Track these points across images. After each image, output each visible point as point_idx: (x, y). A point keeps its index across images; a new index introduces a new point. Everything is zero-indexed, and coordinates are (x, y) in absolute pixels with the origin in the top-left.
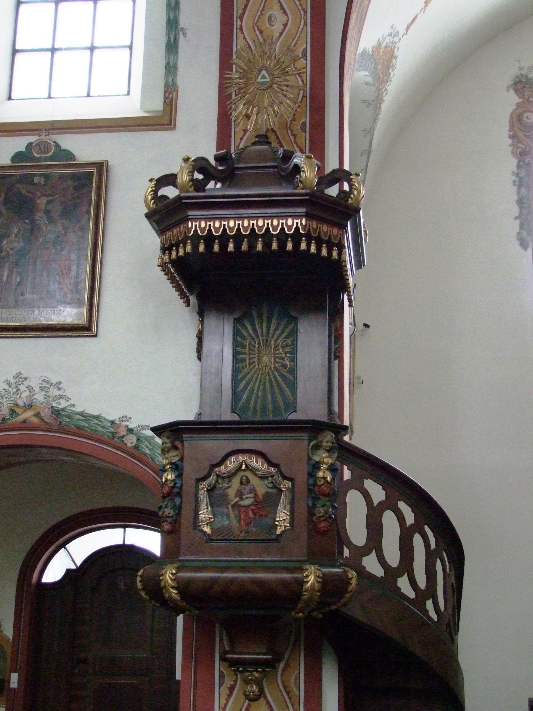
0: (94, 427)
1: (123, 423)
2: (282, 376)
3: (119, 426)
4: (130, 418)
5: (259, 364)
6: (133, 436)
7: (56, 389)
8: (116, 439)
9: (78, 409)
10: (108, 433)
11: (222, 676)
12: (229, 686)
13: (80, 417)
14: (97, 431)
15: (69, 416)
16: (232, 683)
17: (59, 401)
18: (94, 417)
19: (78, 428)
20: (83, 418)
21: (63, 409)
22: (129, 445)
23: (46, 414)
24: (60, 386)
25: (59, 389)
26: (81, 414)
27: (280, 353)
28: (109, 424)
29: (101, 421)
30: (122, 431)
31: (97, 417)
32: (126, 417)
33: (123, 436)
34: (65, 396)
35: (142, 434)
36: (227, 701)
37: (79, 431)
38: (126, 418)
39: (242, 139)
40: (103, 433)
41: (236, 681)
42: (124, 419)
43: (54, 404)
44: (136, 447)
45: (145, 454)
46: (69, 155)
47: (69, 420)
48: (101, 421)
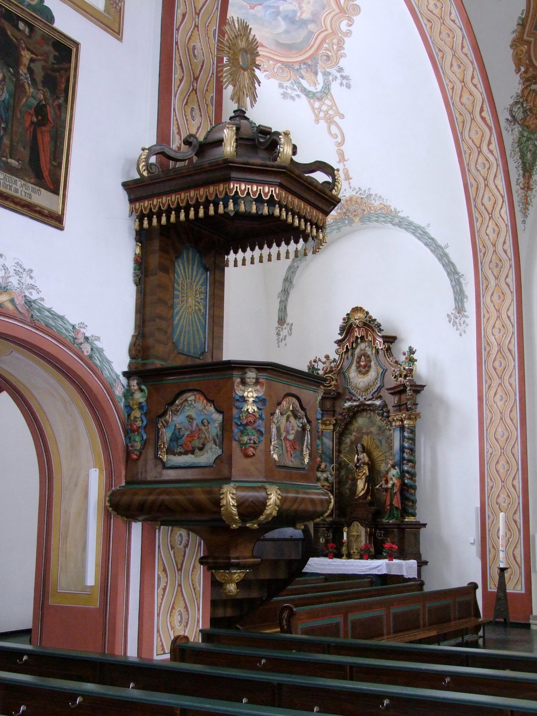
0: (59, 328)
1: (81, 329)
2: (199, 319)
3: (78, 332)
4: (86, 326)
5: (186, 303)
6: (88, 344)
7: (28, 277)
8: (75, 345)
9: (47, 304)
10: (70, 337)
11: (159, 578)
12: (163, 587)
13: (47, 313)
14: (62, 333)
15: (39, 310)
16: (165, 584)
17: (31, 290)
18: (59, 317)
20: (50, 315)
21: (34, 301)
22: (86, 354)
23: (19, 301)
24: (31, 275)
25: (31, 278)
26: (49, 311)
27: (197, 298)
28: (71, 328)
29: (65, 323)
31: (62, 318)
32: (83, 324)
33: (82, 343)
34: (36, 287)
35: (95, 344)
36: (162, 599)
37: (47, 330)
38: (83, 325)
39: (179, 87)
40: (67, 337)
41: (167, 583)
42: (82, 325)
43: (27, 294)
44: (91, 357)
45: (96, 365)
47: (39, 315)
48: (65, 323)
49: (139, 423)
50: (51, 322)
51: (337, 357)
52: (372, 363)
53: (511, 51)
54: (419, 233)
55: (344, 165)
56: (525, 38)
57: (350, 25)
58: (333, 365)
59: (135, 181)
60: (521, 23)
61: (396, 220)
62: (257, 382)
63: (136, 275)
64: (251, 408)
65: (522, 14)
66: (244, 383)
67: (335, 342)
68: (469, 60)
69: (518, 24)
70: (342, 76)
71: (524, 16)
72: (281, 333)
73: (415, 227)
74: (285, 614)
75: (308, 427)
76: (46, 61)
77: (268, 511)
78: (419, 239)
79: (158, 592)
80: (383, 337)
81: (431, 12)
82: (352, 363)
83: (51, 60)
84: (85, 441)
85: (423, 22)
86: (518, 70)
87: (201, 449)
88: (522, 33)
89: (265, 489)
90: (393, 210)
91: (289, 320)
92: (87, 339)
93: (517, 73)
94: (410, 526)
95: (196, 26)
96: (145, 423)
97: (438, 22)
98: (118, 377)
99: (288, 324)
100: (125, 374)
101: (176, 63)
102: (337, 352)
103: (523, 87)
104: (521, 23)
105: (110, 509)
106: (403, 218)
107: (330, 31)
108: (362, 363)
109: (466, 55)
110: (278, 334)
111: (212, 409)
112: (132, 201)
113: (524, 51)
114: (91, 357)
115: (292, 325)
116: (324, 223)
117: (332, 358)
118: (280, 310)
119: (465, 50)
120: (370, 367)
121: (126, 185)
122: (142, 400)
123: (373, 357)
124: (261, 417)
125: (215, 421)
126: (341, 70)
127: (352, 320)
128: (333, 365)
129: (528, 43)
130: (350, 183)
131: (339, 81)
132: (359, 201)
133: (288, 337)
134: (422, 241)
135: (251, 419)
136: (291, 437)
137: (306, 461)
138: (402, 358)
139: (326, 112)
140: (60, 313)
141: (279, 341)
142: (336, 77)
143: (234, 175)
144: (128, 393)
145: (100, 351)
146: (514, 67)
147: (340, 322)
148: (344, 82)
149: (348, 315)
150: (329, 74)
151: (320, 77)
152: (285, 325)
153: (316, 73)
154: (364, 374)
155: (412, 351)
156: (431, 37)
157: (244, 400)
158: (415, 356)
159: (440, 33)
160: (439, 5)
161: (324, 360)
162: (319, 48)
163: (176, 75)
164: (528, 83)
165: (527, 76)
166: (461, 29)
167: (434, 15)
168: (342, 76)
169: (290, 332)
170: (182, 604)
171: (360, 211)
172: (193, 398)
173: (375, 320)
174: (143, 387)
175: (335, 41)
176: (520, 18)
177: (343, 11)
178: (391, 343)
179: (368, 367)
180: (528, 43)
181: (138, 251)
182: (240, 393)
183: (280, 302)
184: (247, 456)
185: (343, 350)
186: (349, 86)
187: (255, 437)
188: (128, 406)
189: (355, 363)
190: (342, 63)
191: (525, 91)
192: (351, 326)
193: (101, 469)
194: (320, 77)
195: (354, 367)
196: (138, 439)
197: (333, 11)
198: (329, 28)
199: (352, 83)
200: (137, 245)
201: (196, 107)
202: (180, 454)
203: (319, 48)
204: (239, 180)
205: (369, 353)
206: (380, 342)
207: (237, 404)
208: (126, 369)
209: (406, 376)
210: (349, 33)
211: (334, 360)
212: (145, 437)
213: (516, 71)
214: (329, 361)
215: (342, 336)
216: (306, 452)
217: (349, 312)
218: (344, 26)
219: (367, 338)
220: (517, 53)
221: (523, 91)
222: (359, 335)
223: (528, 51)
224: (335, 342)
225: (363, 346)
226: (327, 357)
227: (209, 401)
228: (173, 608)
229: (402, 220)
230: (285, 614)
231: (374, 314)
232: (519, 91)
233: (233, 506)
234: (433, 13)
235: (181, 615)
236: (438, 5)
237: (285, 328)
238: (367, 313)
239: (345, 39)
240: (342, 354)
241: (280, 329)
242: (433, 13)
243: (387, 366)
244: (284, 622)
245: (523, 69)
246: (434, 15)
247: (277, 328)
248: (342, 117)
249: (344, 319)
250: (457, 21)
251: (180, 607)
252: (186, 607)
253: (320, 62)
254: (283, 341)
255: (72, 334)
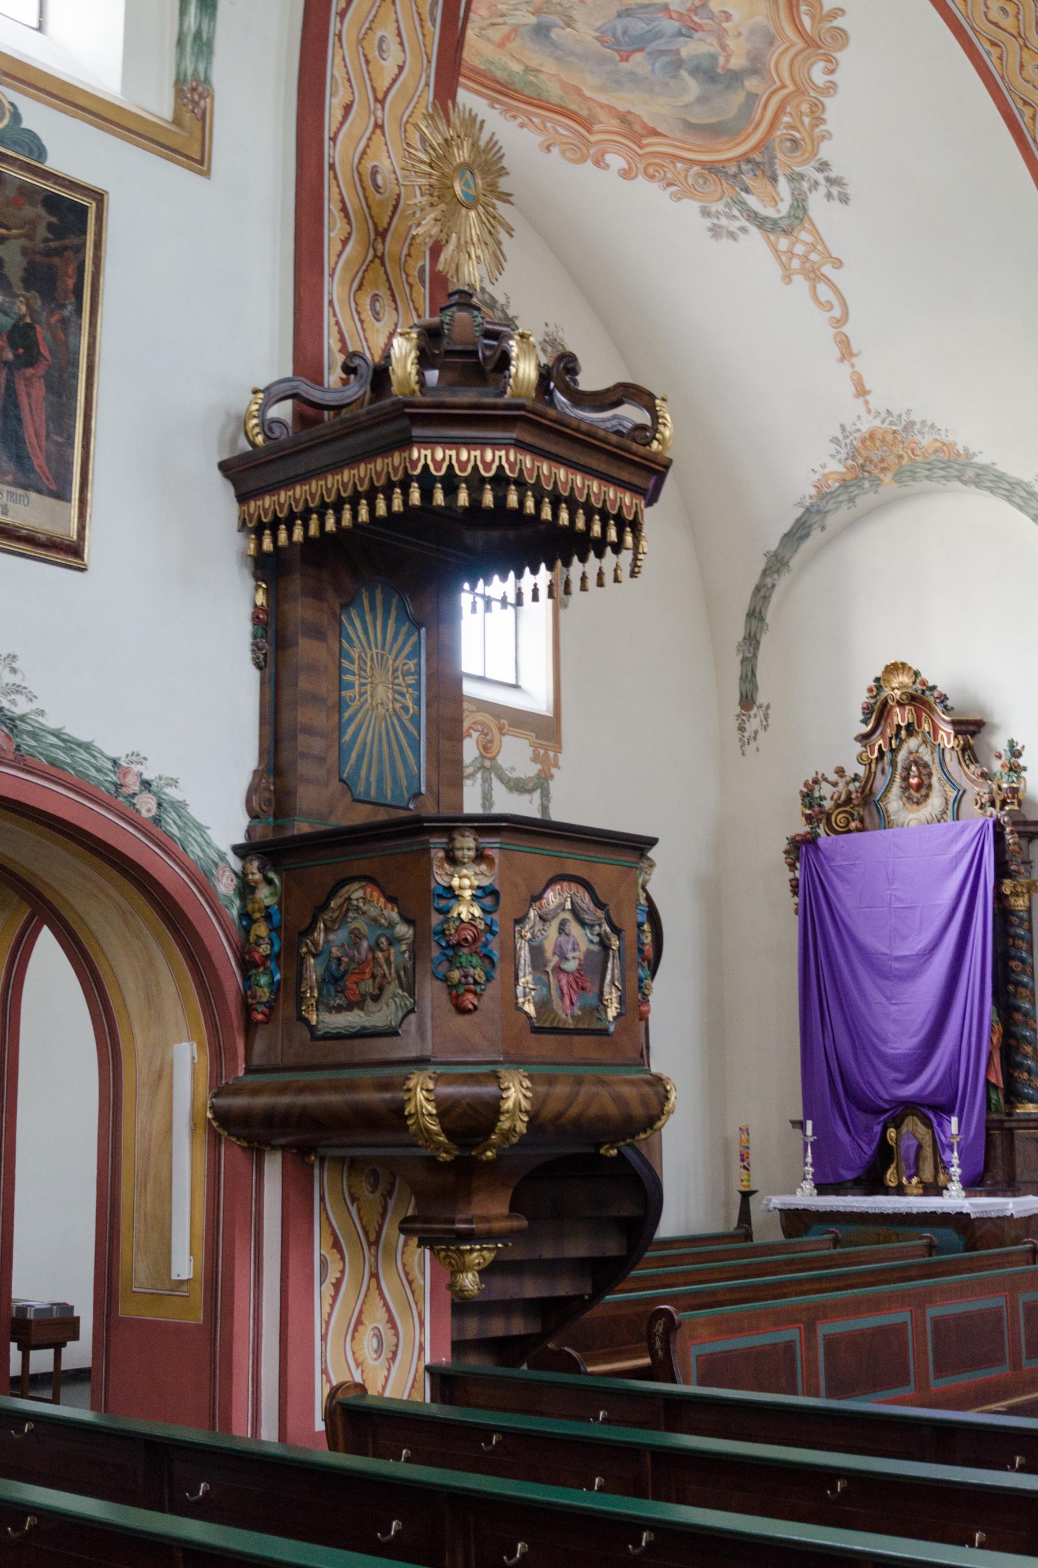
0: (82, 766)
1: (132, 766)
2: (403, 727)
3: (126, 773)
4: (145, 759)
5: (372, 697)
6: (150, 795)
7: (7, 670)
8: (121, 799)
9: (51, 722)
10: (107, 784)
11: (324, 1263)
12: (334, 1281)
14: (88, 776)
15: (34, 735)
16: (338, 1275)
17: (13, 696)
18: (80, 745)
19: (53, 763)
20: (62, 744)
21: (23, 718)
22: (145, 814)
24: (14, 665)
25: (14, 671)
26: (57, 734)
27: (400, 685)
28: (109, 765)
29: (94, 757)
30: (133, 785)
31: (87, 747)
32: (138, 755)
33: (134, 795)
34: (25, 688)
35: (165, 794)
36: (332, 1306)
37: (53, 771)
38: (137, 758)
39: (339, 256)
40: (100, 782)
41: (342, 1272)
42: (134, 758)
44: (157, 820)
45: (171, 836)
46: (35, 147)
47: (34, 743)
48: (94, 757)
49: (264, 949)
50: (62, 756)
51: (861, 771)
52: (934, 780)
54: (1021, 497)
55: (853, 366)
57: (832, 72)
58: (852, 787)
59: (244, 457)
61: (970, 473)
62: (480, 857)
63: (256, 648)
64: (466, 910)
66: (452, 860)
67: (856, 739)
70: (828, 180)
72: (747, 726)
73: (1010, 484)
74: (659, 1327)
75: (615, 943)
76: (29, 237)
77: (505, 1124)
78: (1020, 508)
79: (322, 1293)
80: (954, 723)
81: (996, 25)
82: (892, 781)
83: (42, 232)
84: (169, 988)
85: (982, 46)
87: (376, 998)
89: (496, 1077)
90: (962, 452)
91: (761, 698)
92: (146, 784)
94: (1023, 1124)
95: (379, 126)
96: (276, 948)
97: (1013, 46)
98: (222, 856)
99: (760, 707)
100: (237, 850)
101: (331, 207)
102: (860, 759)
105: (215, 1124)
106: (983, 467)
107: (791, 88)
108: (914, 781)
110: (742, 729)
111: (395, 915)
112: (242, 498)
114: (157, 820)
115: (768, 707)
116: (636, 513)
117: (850, 774)
118: (743, 679)
120: (930, 786)
121: (224, 467)
122: (268, 902)
123: (935, 769)
124: (489, 929)
125: (400, 940)
126: (824, 166)
127: (887, 692)
128: (852, 787)
130: (866, 402)
131: (822, 190)
132: (889, 438)
133: (761, 734)
134: (1028, 514)
135: (469, 935)
136: (571, 966)
137: (612, 1012)
138: (997, 766)
139: (805, 258)
140: (83, 737)
141: (744, 743)
142: (816, 183)
143: (417, 432)
144: (245, 889)
145: (179, 807)
147: (862, 697)
148: (835, 190)
149: (877, 680)
150: (802, 177)
151: (784, 187)
152: (755, 708)
153: (774, 179)
154: (918, 803)
155: (1016, 753)
156: (1002, 78)
157: (451, 893)
158: (1021, 761)
159: (1022, 66)
160: (1010, 8)
161: (833, 777)
162: (773, 125)
163: (334, 229)
167: (1004, 30)
168: (828, 180)
169: (765, 723)
170: (381, 1314)
171: (892, 460)
172: (360, 894)
173: (933, 688)
174: (272, 875)
175: (805, 107)
177: (811, 43)
178: (973, 734)
179: (924, 788)
181: (261, 599)
182: (443, 880)
183: (742, 662)
184: (462, 1010)
185: (872, 753)
186: (844, 199)
187: (479, 974)
188: (245, 915)
189: (898, 779)
190: (826, 151)
192: (885, 703)
193: (200, 1045)
194: (784, 187)
195: (896, 789)
196: (263, 980)
197: (793, 45)
198: (788, 82)
199: (850, 190)
200: (257, 587)
201: (383, 292)
202: (339, 1009)
203: (773, 125)
204: (429, 442)
205: (927, 758)
206: (949, 735)
207: (442, 903)
208: (240, 839)
209: (1004, 803)
210: (831, 88)
211: (856, 778)
212: (278, 977)
214: (844, 780)
215: (867, 725)
216: (612, 996)
217: (879, 674)
218: (818, 74)
219: (920, 726)
222: (903, 721)
224: (856, 739)
225: (913, 743)
226: (840, 772)
227: (391, 899)
228: (359, 1322)
229: (979, 472)
230: (659, 1327)
231: (931, 677)
233: (430, 1115)
234: (1000, 28)
235: (379, 1337)
236: (1008, 8)
237: (755, 715)
238: (916, 674)
239: (826, 101)
240: (870, 764)
241: (745, 718)
242: (1000, 28)
243: (965, 783)
244: (658, 1344)
246: (1004, 30)
247: (738, 716)
248: (838, 264)
249: (870, 690)
251: (376, 1318)
252: (391, 1320)
253: (779, 154)
254: (752, 742)
255: (113, 777)
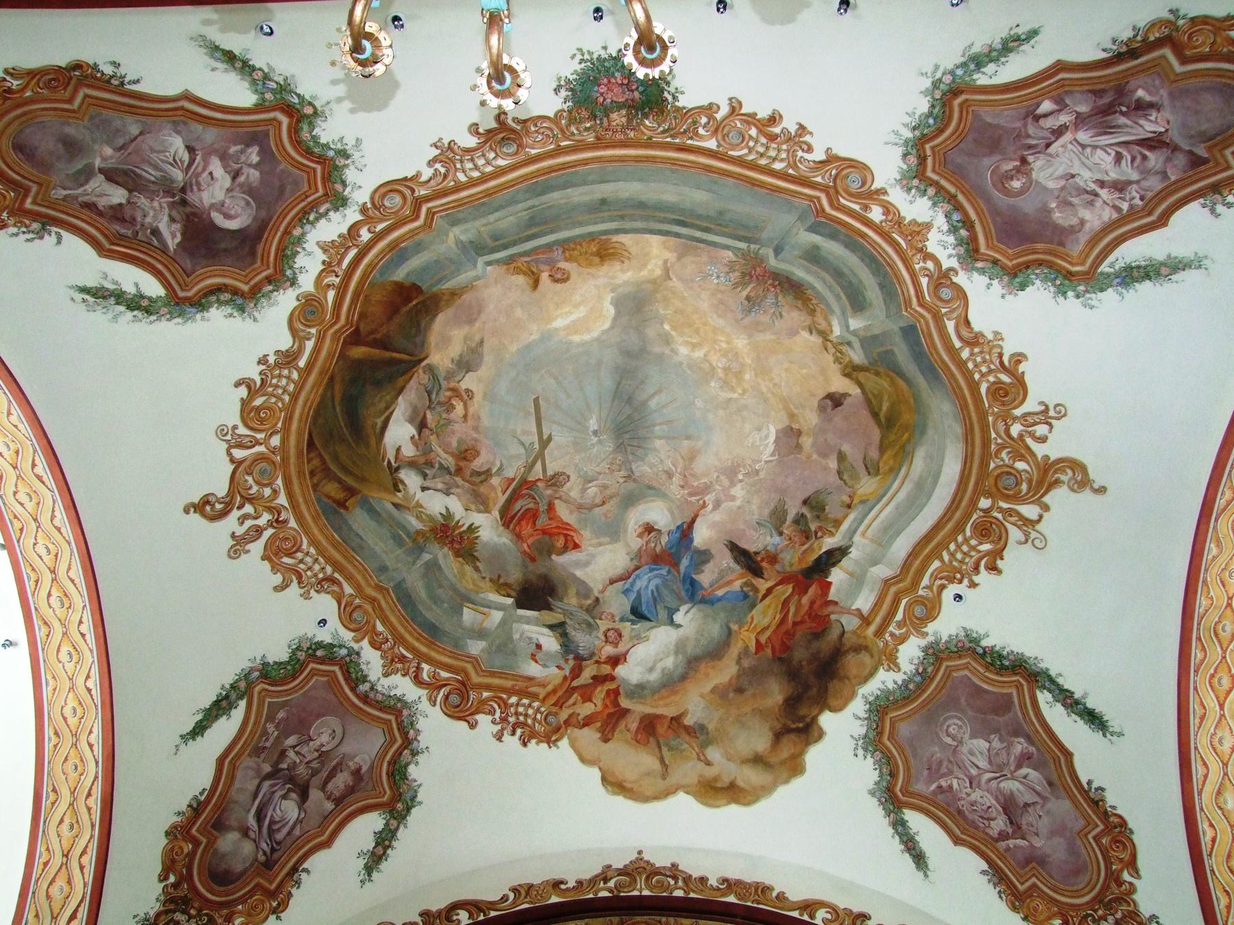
53: (164, 841)
56: (194, 831)
60: (195, 806)
65: (201, 794)
68: (91, 819)
69: (190, 806)
71: (202, 798)
81: (65, 719)
85: (48, 732)
86: (163, 877)
88: (191, 821)
93: (161, 881)
97: (68, 740)
103: (162, 908)
104: (195, 806)
109: (89, 809)
113: (186, 851)
119: (91, 802)
129: (196, 843)
146: (159, 868)
156: (49, 762)
164: (172, 907)
165: (176, 894)
166: (97, 763)
167: (68, 726)
176: (195, 798)
180: (196, 843)
191: (163, 917)
213: (160, 876)
220: (172, 849)
221: (158, 915)
223: (192, 855)
232: (152, 913)
234: (66, 722)
242: (66, 722)
245: (172, 879)
246: (68, 726)
250: (95, 748)
